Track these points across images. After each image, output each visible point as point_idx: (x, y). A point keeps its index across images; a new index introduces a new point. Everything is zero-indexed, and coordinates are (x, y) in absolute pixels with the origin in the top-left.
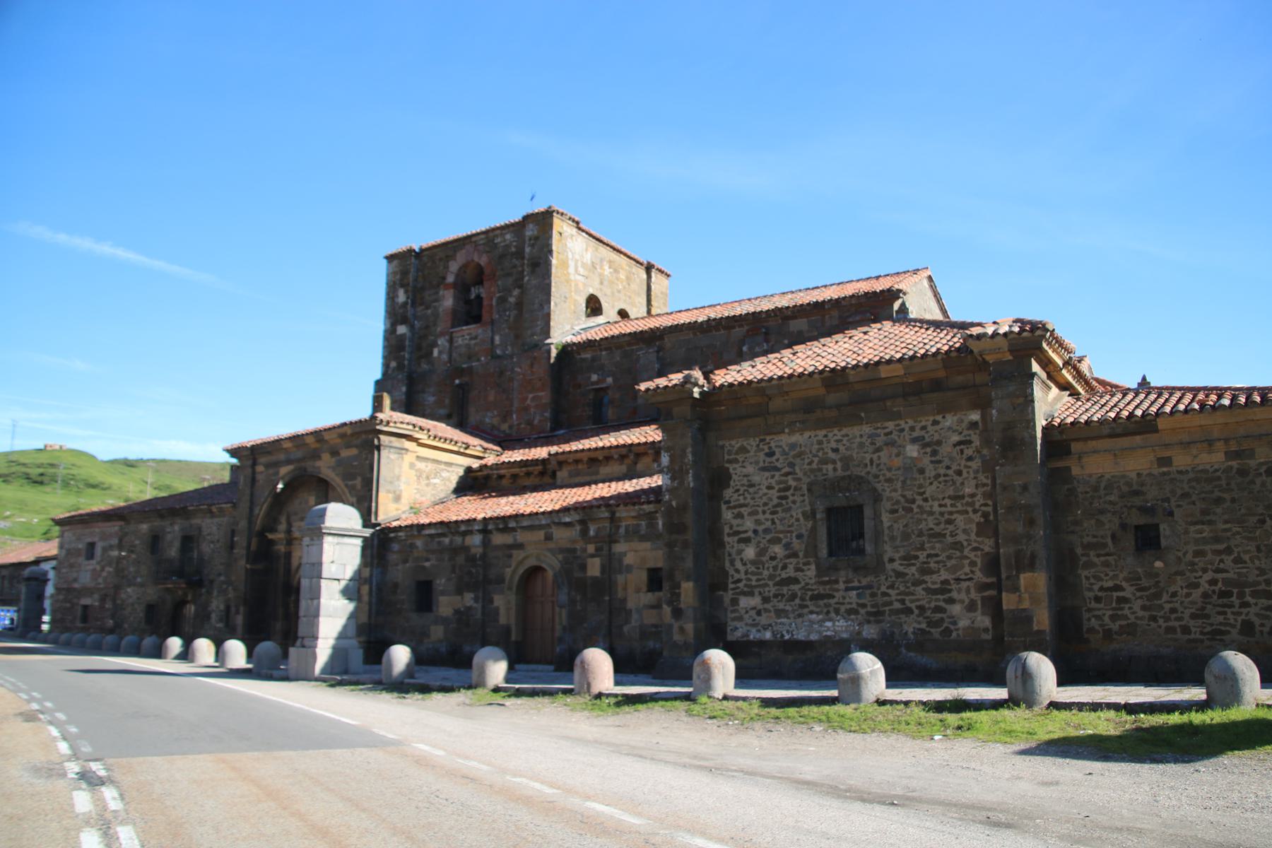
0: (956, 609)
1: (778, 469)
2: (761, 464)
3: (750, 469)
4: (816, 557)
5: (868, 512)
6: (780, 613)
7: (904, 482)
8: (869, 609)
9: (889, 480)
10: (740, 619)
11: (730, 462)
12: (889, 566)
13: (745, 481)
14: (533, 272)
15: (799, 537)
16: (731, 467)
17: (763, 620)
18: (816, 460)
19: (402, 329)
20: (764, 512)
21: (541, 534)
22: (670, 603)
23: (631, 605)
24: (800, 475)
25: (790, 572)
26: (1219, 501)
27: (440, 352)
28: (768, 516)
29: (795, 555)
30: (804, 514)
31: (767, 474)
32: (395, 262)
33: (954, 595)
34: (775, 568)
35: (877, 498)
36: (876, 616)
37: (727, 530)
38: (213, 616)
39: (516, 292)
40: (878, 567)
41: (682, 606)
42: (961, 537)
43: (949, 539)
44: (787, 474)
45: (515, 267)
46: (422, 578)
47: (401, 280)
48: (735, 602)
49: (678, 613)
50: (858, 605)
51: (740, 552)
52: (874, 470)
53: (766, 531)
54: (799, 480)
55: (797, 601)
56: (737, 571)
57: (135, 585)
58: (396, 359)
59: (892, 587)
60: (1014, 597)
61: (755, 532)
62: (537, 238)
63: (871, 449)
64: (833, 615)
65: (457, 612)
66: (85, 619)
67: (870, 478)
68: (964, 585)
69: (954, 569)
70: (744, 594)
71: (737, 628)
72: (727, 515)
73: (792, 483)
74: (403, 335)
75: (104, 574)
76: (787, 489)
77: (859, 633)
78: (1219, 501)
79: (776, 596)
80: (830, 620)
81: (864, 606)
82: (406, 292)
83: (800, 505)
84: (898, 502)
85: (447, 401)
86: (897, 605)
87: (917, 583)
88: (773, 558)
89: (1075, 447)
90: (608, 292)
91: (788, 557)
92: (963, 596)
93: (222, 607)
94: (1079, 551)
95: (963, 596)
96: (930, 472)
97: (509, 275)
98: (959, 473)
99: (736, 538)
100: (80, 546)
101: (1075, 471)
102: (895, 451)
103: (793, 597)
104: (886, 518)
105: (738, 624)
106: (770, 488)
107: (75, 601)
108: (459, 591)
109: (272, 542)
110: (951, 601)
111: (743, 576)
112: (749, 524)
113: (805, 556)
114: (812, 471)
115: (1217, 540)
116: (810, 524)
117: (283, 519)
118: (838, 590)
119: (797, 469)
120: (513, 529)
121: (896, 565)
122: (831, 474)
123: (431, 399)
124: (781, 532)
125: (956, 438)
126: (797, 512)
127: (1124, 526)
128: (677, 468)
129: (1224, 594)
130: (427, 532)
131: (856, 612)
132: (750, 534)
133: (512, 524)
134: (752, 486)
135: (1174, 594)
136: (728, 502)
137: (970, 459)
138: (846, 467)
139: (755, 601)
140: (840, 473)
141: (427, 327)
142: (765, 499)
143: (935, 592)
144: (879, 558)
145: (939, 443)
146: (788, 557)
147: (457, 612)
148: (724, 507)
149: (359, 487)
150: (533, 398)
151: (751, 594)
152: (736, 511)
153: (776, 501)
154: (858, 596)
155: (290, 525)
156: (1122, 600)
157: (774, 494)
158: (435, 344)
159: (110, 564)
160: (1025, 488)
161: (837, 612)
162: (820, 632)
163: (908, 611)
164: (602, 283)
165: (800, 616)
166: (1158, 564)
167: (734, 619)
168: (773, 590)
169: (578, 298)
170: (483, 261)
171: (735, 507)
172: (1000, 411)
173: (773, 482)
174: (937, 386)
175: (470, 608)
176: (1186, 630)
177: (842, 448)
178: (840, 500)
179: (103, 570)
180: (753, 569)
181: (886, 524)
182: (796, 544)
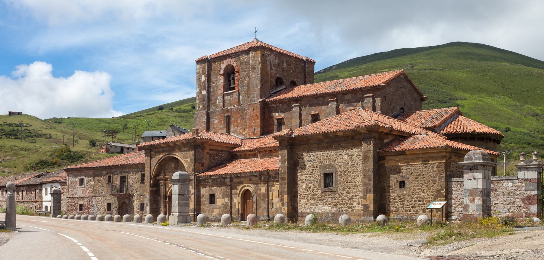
0: (354, 204)
5: (334, 175)
6: (311, 204)
11: (299, 158)
12: (339, 191)
16: (299, 160)
17: (307, 206)
21: (248, 179)
25: (314, 192)
26: (420, 175)
29: (316, 187)
33: (355, 200)
40: (336, 192)
42: (357, 183)
43: (354, 184)
48: (300, 201)
49: (283, 204)
52: (336, 163)
60: (365, 200)
68: (357, 197)
69: (354, 193)
73: (315, 166)
78: (420, 175)
81: (333, 202)
86: (341, 202)
87: (346, 196)
88: (310, 188)
89: (387, 158)
92: (357, 200)
94: (386, 188)
95: (357, 200)
96: (350, 164)
98: (357, 164)
101: (386, 165)
103: (315, 200)
104: (338, 176)
106: (310, 167)
108: (223, 198)
109: (159, 180)
110: (354, 201)
115: (418, 186)
117: (163, 172)
120: (240, 177)
122: (325, 163)
125: (357, 154)
126: (316, 174)
127: (397, 181)
129: (419, 201)
130: (212, 177)
133: (239, 175)
135: (408, 201)
137: (360, 160)
138: (329, 162)
140: (327, 163)
143: (350, 199)
144: (337, 188)
145: (352, 155)
155: (165, 173)
156: (396, 202)
160: (369, 170)
163: (344, 204)
165: (317, 205)
166: (405, 192)
168: (310, 198)
172: (364, 148)
174: (352, 138)
175: (227, 203)
176: (410, 211)
178: (327, 171)
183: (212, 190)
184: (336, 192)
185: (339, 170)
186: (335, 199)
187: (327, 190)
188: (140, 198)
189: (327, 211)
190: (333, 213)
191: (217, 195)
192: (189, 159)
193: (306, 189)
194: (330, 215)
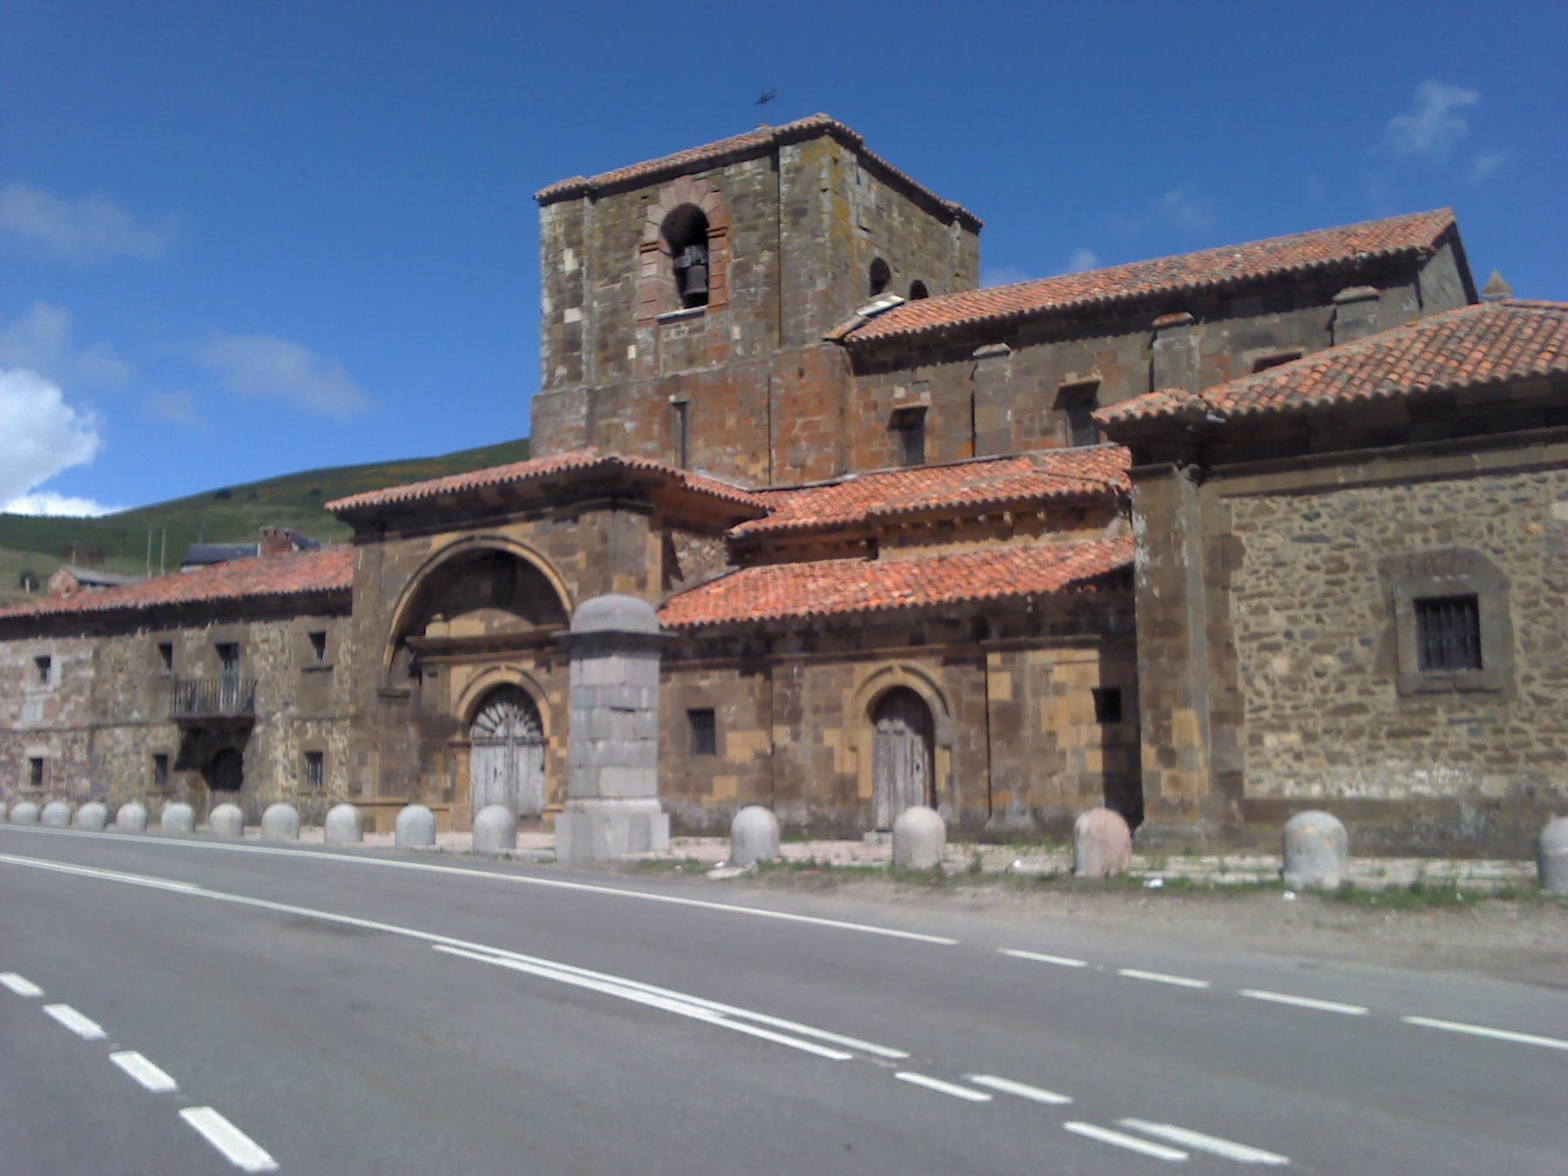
1: (1324, 539)
2: (1297, 532)
3: (1275, 539)
4: (1398, 671)
5: (1486, 606)
6: (1333, 758)
7: (1547, 561)
8: (1491, 753)
9: (1522, 558)
10: (1268, 765)
11: (1242, 528)
12: (1522, 690)
13: (1269, 558)
14: (795, 224)
15: (1364, 642)
16: (1243, 537)
17: (1305, 768)
18: (1393, 526)
19: (572, 315)
20: (1303, 605)
22: (1154, 741)
23: (1063, 742)
24: (1364, 546)
25: (1352, 695)
27: (640, 353)
28: (1309, 610)
29: (1360, 669)
30: (1374, 608)
31: (1308, 547)
32: (554, 207)
34: (1324, 690)
35: (1504, 585)
36: (1504, 759)
37: (1238, 631)
38: (279, 770)
39: (766, 256)
41: (1175, 744)
44: (1342, 547)
45: (761, 215)
46: (697, 704)
47: (566, 235)
48: (1256, 740)
50: (1472, 746)
51: (1262, 665)
52: (1495, 542)
53: (1307, 634)
54: (1362, 556)
55: (1365, 740)
56: (1259, 694)
57: (128, 724)
58: (564, 362)
59: (1529, 719)
61: (1288, 635)
62: (798, 170)
63: (1489, 509)
64: (1428, 761)
65: (759, 755)
66: (37, 778)
67: (1489, 554)
70: (1272, 728)
71: (1259, 780)
72: (1238, 608)
74: (577, 324)
75: (70, 707)
76: (1344, 568)
77: (1473, 789)
79: (1327, 731)
80: (1424, 768)
81: (1481, 748)
82: (577, 255)
83: (1364, 595)
84: (1536, 591)
85: (656, 428)
86: (1539, 748)
90: (898, 253)
91: (1347, 672)
93: (294, 754)
97: (753, 228)
99: (1255, 645)
100: (22, 662)
102: (1530, 512)
103: (1356, 733)
105: (1264, 774)
107: (15, 750)
111: (1270, 702)
112: (1277, 620)
113: (1380, 668)
114: (1387, 542)
116: (1383, 626)
118: (1434, 724)
119: (1360, 541)
121: (1536, 687)
123: (629, 426)
124: (1334, 635)
126: (1361, 605)
128: (1160, 537)
131: (1467, 757)
132: (1280, 638)
134: (1280, 564)
136: (1240, 589)
138: (1442, 540)
139: (1293, 738)
140: (1435, 546)
141: (615, 312)
142: (1303, 586)
146: (1347, 672)
147: (759, 755)
148: (1232, 596)
149: (582, 565)
150: (805, 427)
151: (1285, 728)
152: (1255, 602)
153: (1322, 588)
154: (1472, 732)
157: (1319, 578)
158: (628, 341)
159: (79, 691)
161: (1435, 757)
162: (1407, 787)
164: (890, 241)
165: (1370, 762)
167: (1254, 766)
169: (861, 266)
170: (707, 205)
171: (1252, 597)
173: (1317, 560)
177: (1436, 506)
178: (1436, 586)
179: (65, 699)
180: (1286, 690)
181: (1517, 621)
182: (1360, 651)
183: (698, 690)
184: (1497, 693)
185: (1515, 579)
186: (1499, 731)
187: (1438, 685)
188: (300, 732)
189: (1449, 791)
190: (1491, 805)
191: (726, 713)
192: (580, 558)
193: (1292, 682)
194: (1469, 814)
